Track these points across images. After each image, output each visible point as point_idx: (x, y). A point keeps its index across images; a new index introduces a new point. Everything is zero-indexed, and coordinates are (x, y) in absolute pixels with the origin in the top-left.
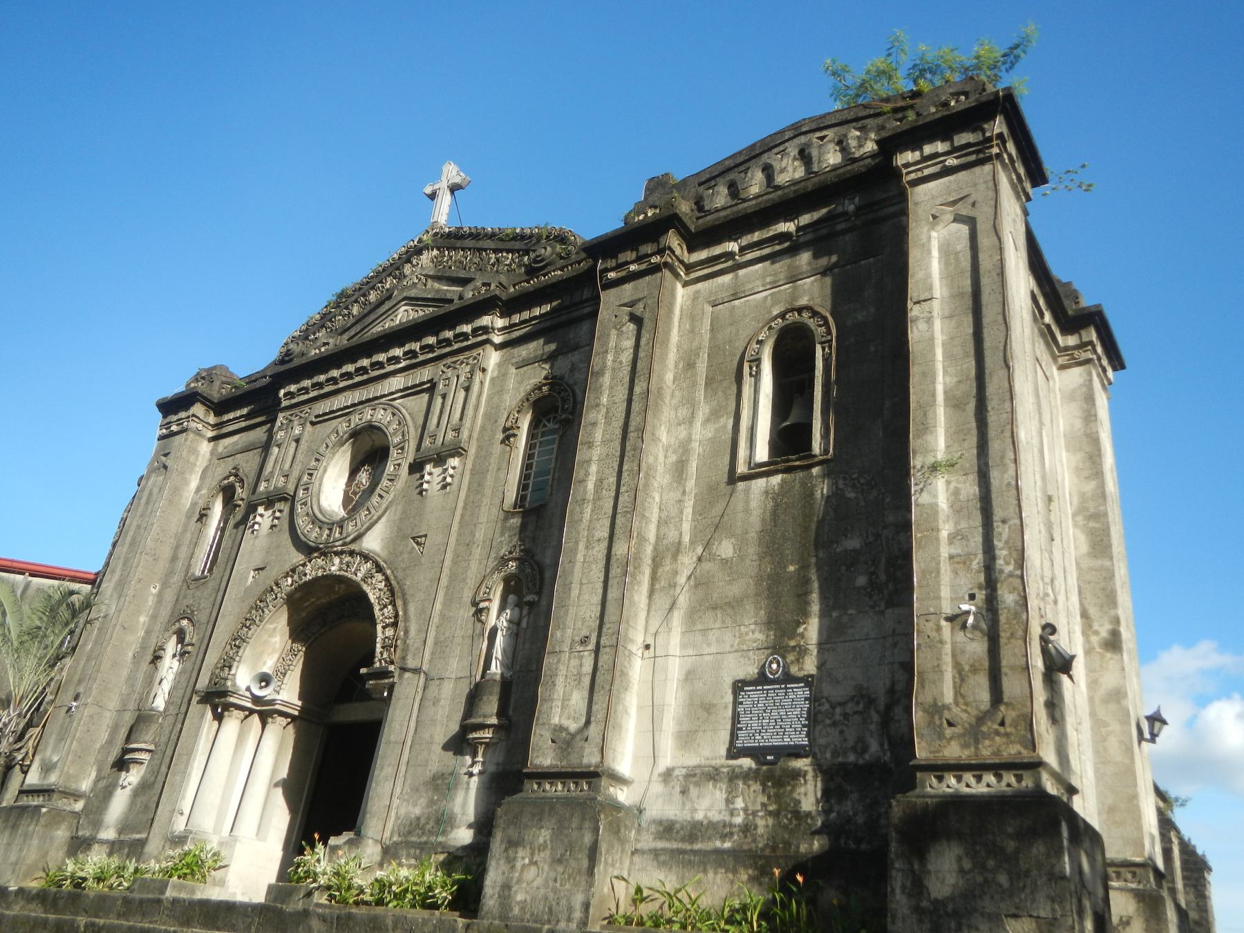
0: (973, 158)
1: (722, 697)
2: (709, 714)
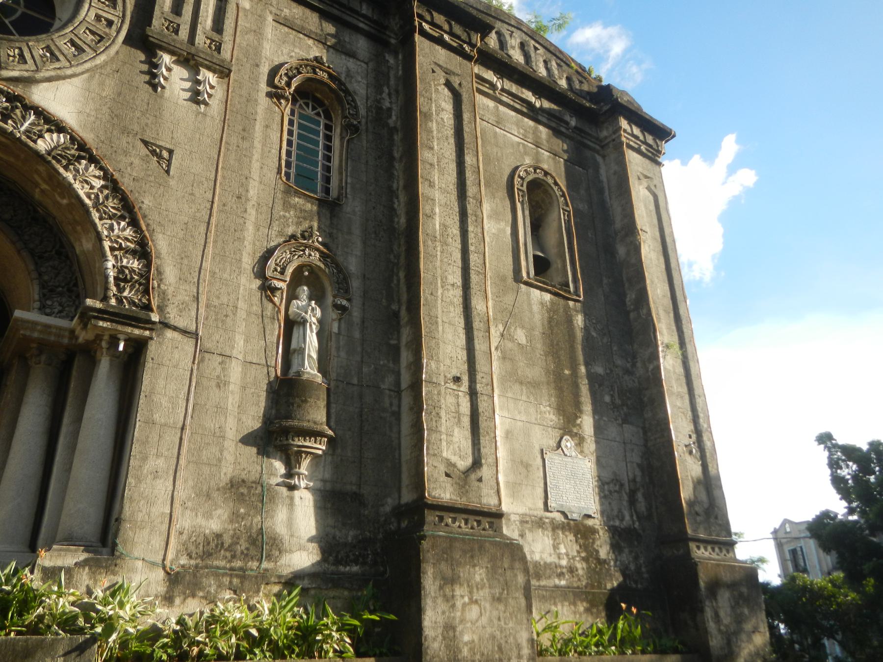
0: (650, 154)
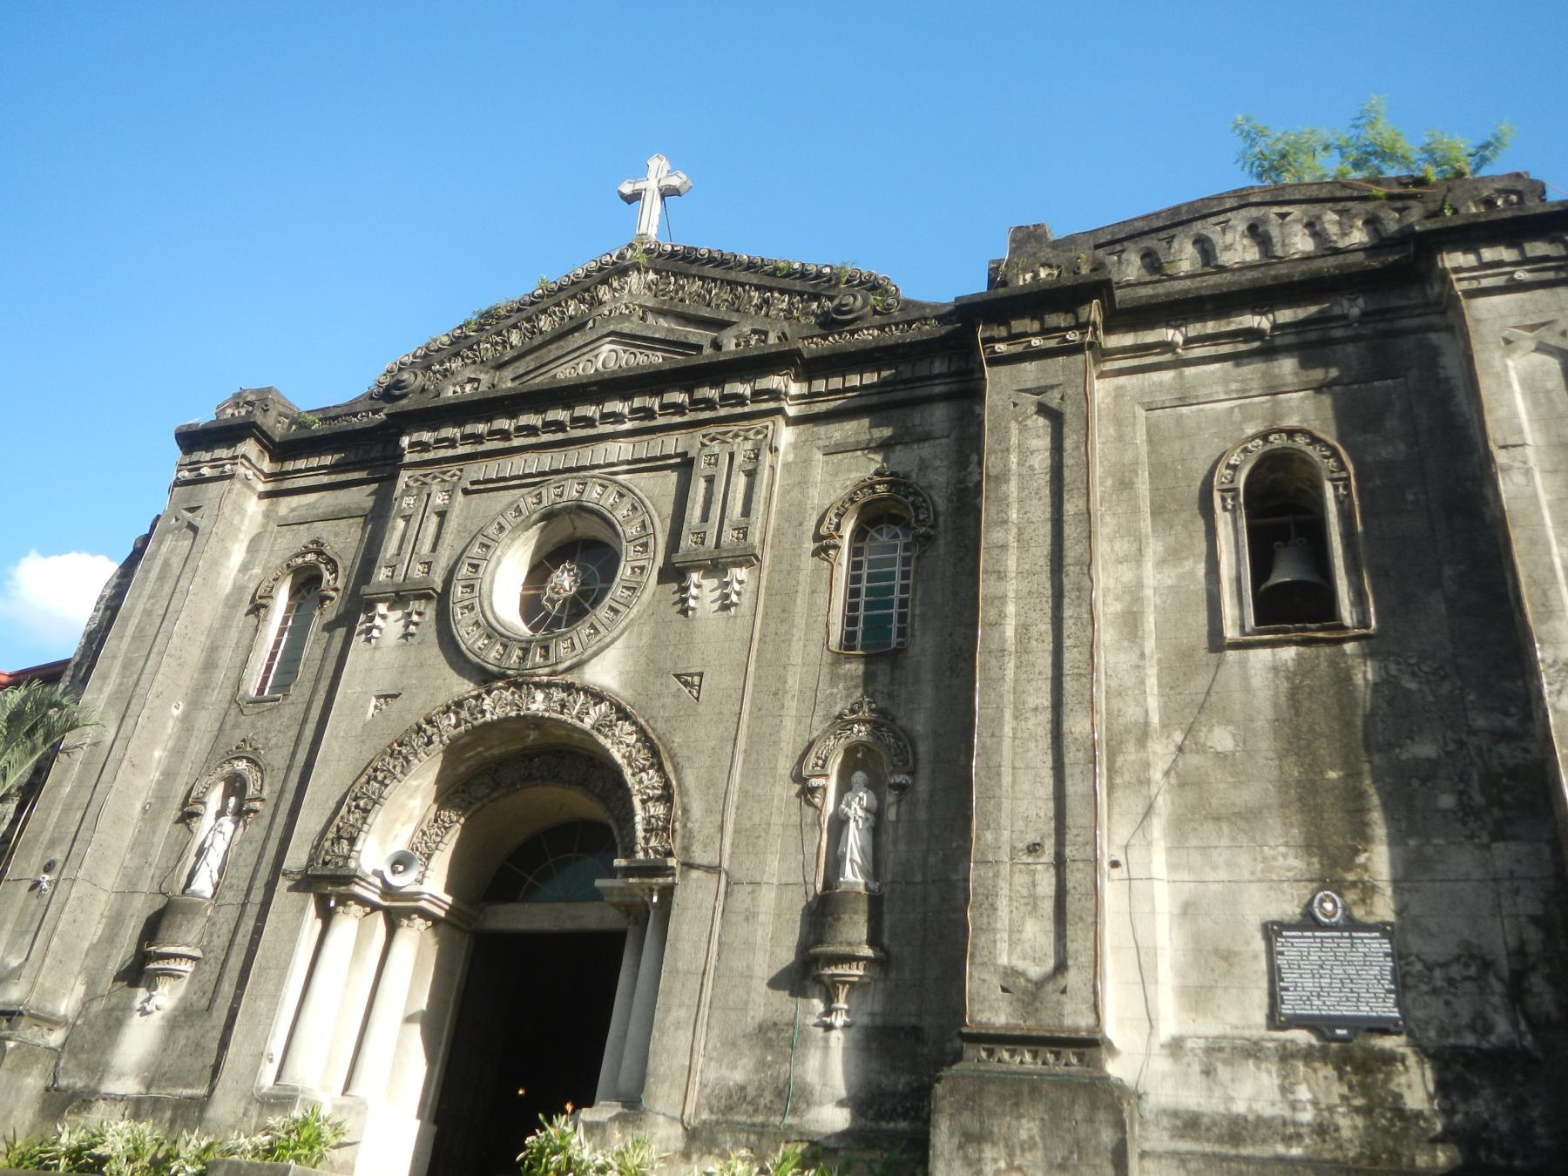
0: (1551, 275)
1: (1247, 943)
2: (1231, 965)
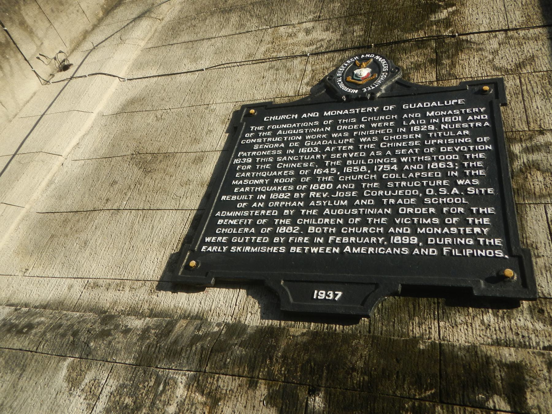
1: (196, 141)
2: (147, 172)
